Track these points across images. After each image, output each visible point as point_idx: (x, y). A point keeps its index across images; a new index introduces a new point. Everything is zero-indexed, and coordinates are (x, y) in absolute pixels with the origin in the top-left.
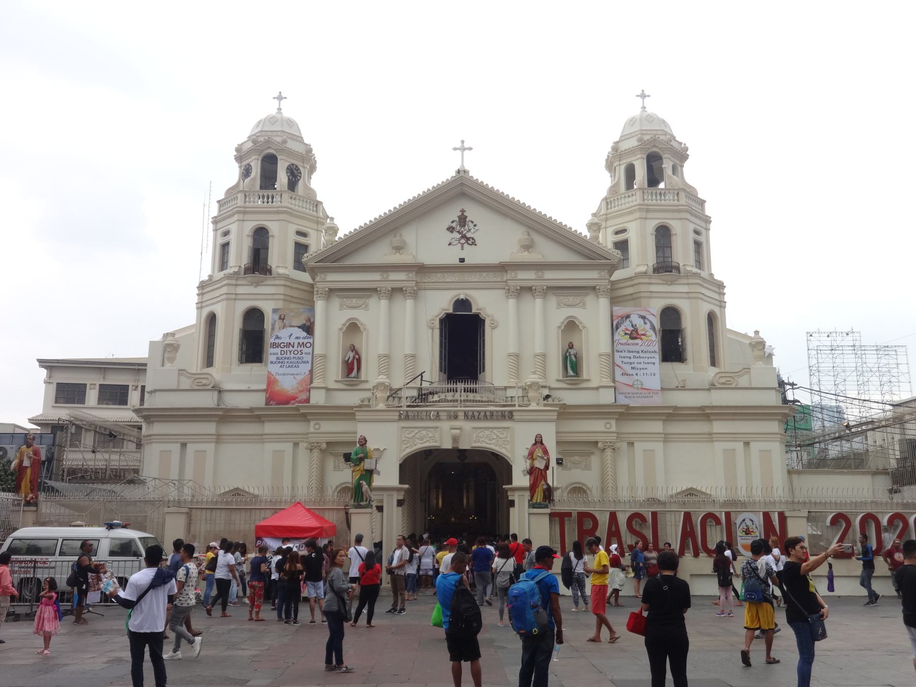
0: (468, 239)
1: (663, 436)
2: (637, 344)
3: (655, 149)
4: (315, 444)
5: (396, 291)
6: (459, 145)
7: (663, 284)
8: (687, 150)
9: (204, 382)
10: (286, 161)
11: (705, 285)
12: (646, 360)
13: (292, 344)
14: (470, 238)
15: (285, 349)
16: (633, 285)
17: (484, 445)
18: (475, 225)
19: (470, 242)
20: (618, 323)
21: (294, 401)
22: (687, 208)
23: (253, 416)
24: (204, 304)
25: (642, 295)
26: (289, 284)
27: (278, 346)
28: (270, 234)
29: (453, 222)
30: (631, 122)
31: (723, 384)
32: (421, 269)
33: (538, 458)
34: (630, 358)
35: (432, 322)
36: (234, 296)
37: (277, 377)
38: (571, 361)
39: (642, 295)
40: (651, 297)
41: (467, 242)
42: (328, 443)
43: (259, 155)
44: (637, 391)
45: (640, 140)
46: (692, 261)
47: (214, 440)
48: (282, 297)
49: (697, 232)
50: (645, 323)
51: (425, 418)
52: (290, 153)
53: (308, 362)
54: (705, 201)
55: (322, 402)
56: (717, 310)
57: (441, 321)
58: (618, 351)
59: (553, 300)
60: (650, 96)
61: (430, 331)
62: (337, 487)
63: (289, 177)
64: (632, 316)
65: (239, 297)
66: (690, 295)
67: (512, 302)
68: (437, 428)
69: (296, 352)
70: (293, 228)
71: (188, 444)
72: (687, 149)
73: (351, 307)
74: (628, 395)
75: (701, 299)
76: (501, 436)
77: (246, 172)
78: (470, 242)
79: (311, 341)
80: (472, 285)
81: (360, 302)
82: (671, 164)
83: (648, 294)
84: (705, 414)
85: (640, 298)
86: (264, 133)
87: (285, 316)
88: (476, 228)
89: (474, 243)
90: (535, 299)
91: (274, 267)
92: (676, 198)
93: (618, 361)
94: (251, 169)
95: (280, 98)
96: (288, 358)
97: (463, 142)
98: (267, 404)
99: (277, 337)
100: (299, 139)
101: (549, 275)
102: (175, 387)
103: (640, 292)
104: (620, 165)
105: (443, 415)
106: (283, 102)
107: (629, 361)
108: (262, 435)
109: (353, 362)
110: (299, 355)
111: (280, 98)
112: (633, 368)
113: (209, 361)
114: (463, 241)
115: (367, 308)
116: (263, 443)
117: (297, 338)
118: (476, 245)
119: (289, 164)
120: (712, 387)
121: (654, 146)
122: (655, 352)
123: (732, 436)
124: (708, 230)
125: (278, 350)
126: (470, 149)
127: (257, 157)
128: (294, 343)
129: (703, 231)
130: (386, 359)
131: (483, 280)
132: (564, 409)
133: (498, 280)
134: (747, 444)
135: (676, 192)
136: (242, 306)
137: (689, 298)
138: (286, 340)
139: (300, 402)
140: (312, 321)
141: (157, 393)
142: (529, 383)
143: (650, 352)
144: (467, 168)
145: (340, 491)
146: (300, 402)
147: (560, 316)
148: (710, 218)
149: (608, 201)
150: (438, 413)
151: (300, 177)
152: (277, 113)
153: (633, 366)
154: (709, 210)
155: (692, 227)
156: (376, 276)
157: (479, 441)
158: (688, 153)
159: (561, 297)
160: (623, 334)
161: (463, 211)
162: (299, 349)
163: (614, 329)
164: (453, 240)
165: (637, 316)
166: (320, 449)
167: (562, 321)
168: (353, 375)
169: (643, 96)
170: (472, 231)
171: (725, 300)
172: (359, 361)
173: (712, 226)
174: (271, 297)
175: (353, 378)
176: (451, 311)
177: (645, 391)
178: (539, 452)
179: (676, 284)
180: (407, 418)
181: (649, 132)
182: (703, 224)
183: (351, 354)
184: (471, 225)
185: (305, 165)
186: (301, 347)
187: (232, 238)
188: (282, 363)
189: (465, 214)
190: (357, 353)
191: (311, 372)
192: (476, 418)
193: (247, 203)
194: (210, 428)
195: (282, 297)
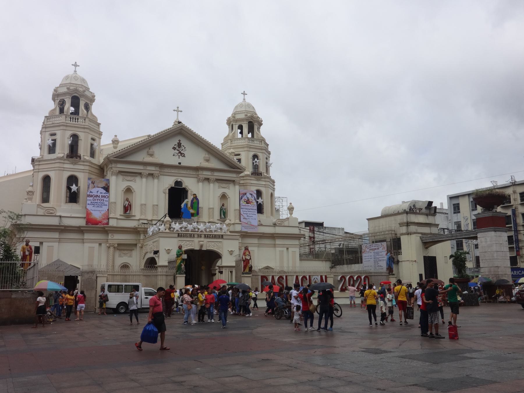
0: (181, 154)
1: (258, 245)
2: (249, 206)
4: (112, 245)
5: (151, 175)
6: (176, 109)
8: (262, 121)
9: (51, 211)
12: (252, 213)
13: (99, 196)
15: (95, 198)
16: (244, 180)
17: (212, 249)
18: (185, 148)
19: (182, 155)
20: (242, 197)
21: (100, 224)
22: (264, 148)
23: (79, 230)
24: (40, 170)
25: (248, 184)
26: (90, 165)
27: (91, 196)
28: (80, 138)
29: (175, 145)
30: (240, 106)
31: (279, 224)
32: (162, 166)
33: (247, 255)
34: (246, 212)
35: (165, 190)
36: (63, 169)
37: (92, 211)
38: (223, 211)
39: (248, 184)
40: (251, 186)
41: (181, 155)
42: (119, 244)
43: (70, 96)
44: (249, 226)
45: (246, 115)
46: (265, 172)
47: (58, 241)
48: (88, 171)
50: (252, 197)
51: (188, 236)
52: (86, 97)
53: (107, 205)
54: (269, 145)
55: (115, 225)
56: (272, 192)
57: (169, 190)
58: (242, 209)
59: (217, 185)
61: (164, 194)
62: (120, 265)
64: (247, 194)
66: (266, 186)
67: (201, 184)
68: (193, 241)
69: (101, 200)
70: (90, 136)
71: (43, 243)
72: (262, 121)
74: (246, 227)
75: (269, 187)
76: (218, 245)
77: (62, 104)
78: (182, 155)
79: (108, 195)
80: (183, 175)
81: (132, 178)
82: (257, 127)
83: (251, 184)
84: (273, 236)
85: (247, 185)
86: (72, 85)
87: (94, 182)
88: (186, 149)
89: (184, 156)
90: (209, 184)
91: (82, 155)
92: (260, 143)
93: (242, 213)
94: (65, 102)
96: (97, 203)
97: (178, 108)
98: (86, 224)
99: (91, 192)
100: (88, 89)
101: (216, 174)
102: (36, 214)
105: (196, 236)
106: (77, 67)
107: (246, 213)
108: (83, 239)
109: (128, 206)
110: (102, 202)
111: (76, 65)
112: (247, 216)
113: (46, 199)
114: (179, 154)
115: (135, 181)
116: (84, 243)
117: (101, 193)
118: (185, 157)
119: (85, 102)
120: (275, 225)
122: (256, 210)
123: (283, 246)
124: (269, 157)
125: (92, 198)
126: (181, 111)
127: (69, 97)
128: (99, 195)
129: (268, 157)
130: (143, 206)
133: (194, 174)
134: (287, 249)
136: (67, 174)
137: (265, 187)
138: (96, 194)
139: (103, 224)
140: (108, 185)
141: (26, 216)
142: (227, 223)
143: (254, 210)
144: (180, 121)
145: (121, 267)
146: (103, 224)
147: (220, 191)
149: (232, 140)
150: (194, 235)
151: (89, 109)
152: (74, 73)
153: (247, 215)
154: (270, 149)
155: (266, 156)
156: (141, 167)
157: (209, 247)
158: (262, 123)
160: (243, 201)
161: (180, 141)
162: (102, 199)
163: (240, 199)
164: (175, 154)
165: (249, 194)
166: (114, 247)
167: (220, 194)
168: (128, 212)
169: (244, 94)
170: (184, 150)
171: (275, 188)
172: (130, 206)
173: (271, 156)
174: (82, 171)
175: (128, 214)
176: (173, 186)
177: (252, 226)
178: (247, 253)
180: (181, 236)
181: (251, 113)
182: (268, 155)
183: (127, 203)
184: (183, 148)
186: (103, 197)
187: (58, 137)
188: (94, 205)
189: (180, 142)
190: (129, 202)
191: (108, 210)
192: (209, 237)
193: (67, 121)
194: (56, 235)
195: (88, 171)
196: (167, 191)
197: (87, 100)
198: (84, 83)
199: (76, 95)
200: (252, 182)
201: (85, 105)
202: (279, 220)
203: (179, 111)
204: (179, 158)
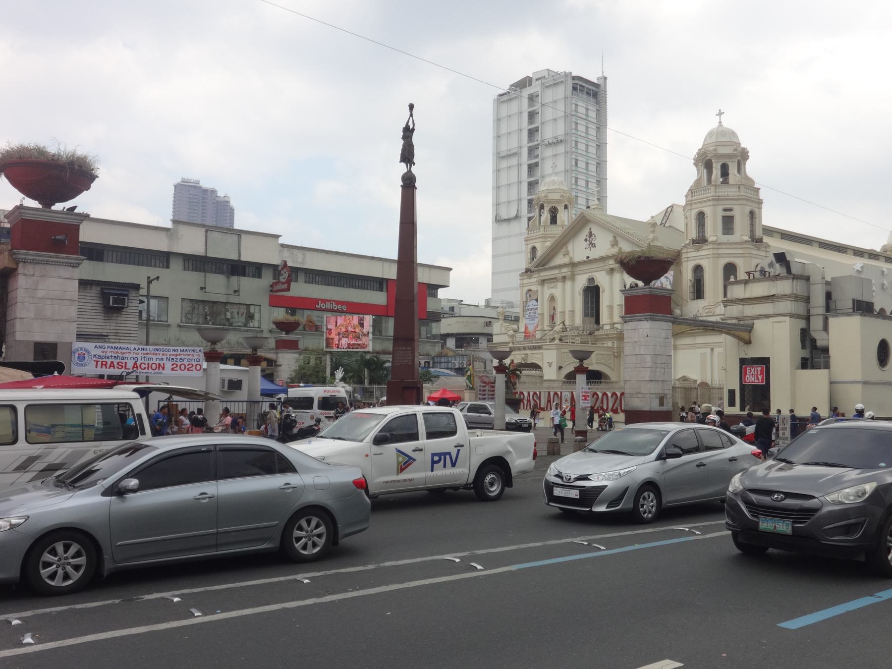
0: (592, 244)
3: (709, 158)
7: (695, 251)
17: (534, 361)
18: (595, 236)
32: (573, 265)
36: (522, 285)
40: (687, 261)
49: (725, 210)
50: (667, 281)
65: (524, 285)
89: (595, 247)
123: (705, 345)
134: (712, 349)
151: (558, 212)
155: (722, 207)
156: (557, 271)
161: (590, 229)
176: (587, 285)
185: (560, 204)
199: (541, 203)
200: (689, 255)
201: (549, 210)
202: (705, 308)
204: (590, 250)
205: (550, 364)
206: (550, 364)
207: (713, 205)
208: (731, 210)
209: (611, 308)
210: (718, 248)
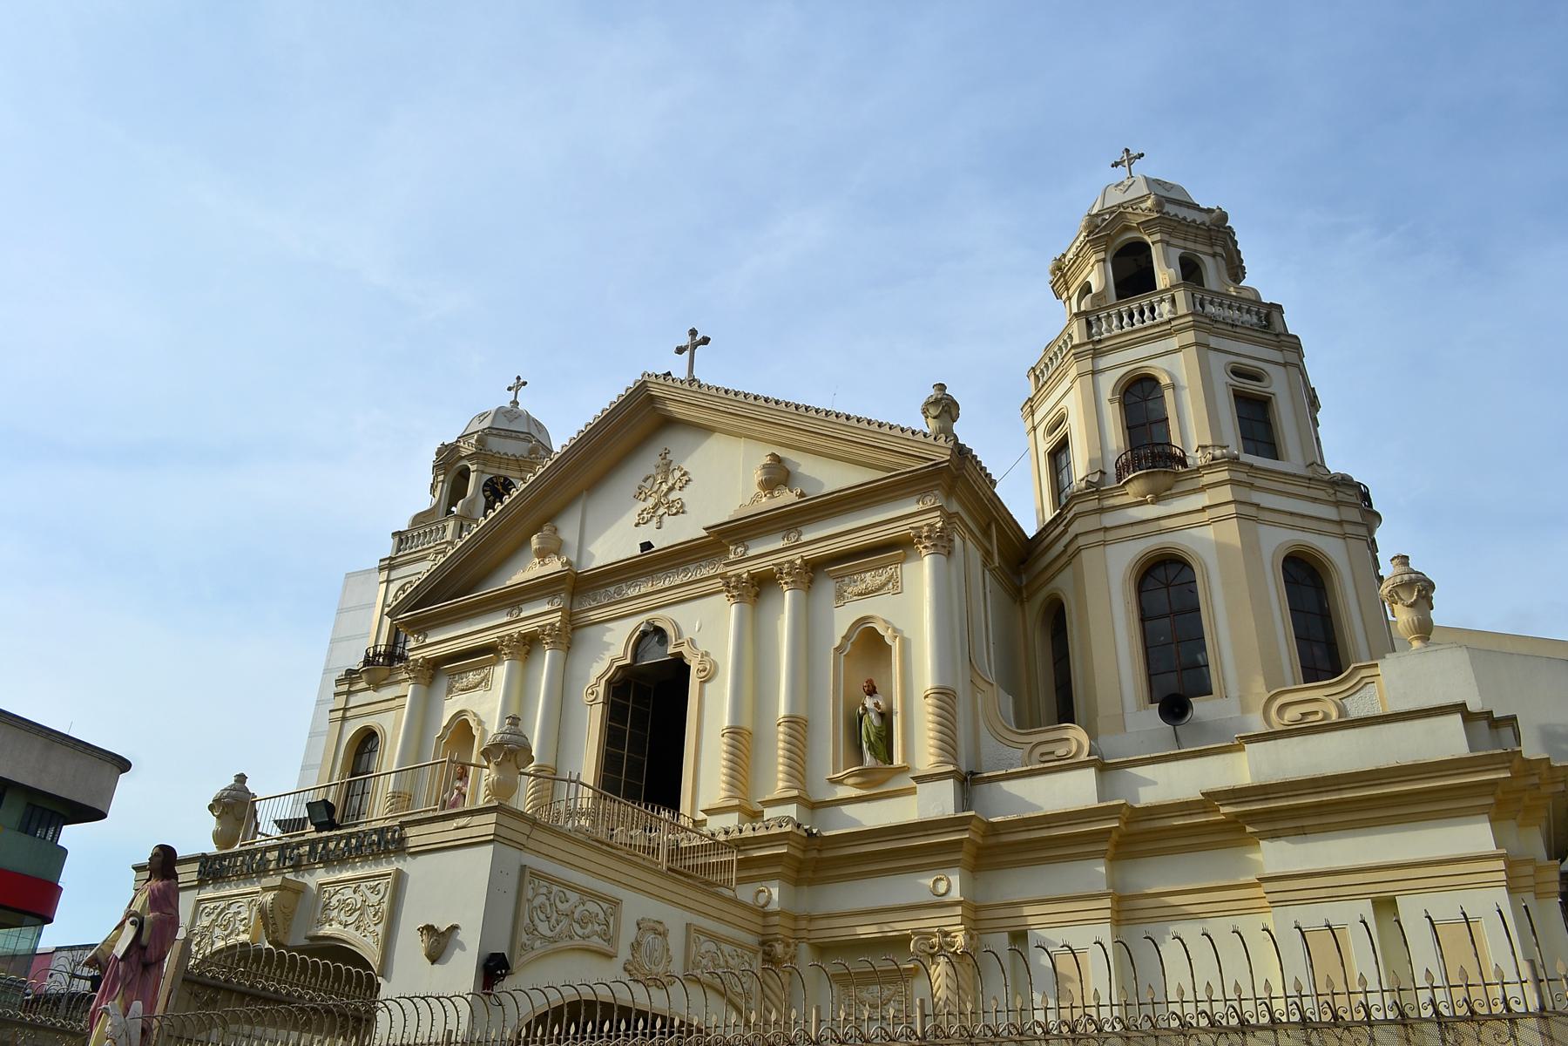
1: (1107, 903)
6: (685, 340)
10: (483, 472)
11: (1258, 482)
14: (673, 501)
29: (645, 481)
35: (590, 691)
39: (1081, 541)
40: (1105, 543)
49: (1237, 372)
56: (1331, 548)
60: (1142, 155)
63: (487, 498)
72: (1224, 217)
73: (463, 690)
82: (1175, 254)
95: (521, 383)
97: (693, 333)
100: (522, 436)
103: (1077, 536)
104: (1069, 298)
111: (521, 383)
121: (1128, 228)
126: (706, 341)
131: (690, 579)
132: (819, 850)
135: (1167, 296)
148: (1296, 337)
149: (1037, 373)
159: (846, 579)
164: (645, 513)
176: (628, 661)
179: (1172, 496)
196: (601, 690)
197: (499, 468)
198: (510, 422)
201: (485, 484)
203: (695, 346)
205: (439, 943)
206: (439, 943)
207: (1196, 344)
208: (1256, 377)
209: (742, 741)
210: (1251, 486)
